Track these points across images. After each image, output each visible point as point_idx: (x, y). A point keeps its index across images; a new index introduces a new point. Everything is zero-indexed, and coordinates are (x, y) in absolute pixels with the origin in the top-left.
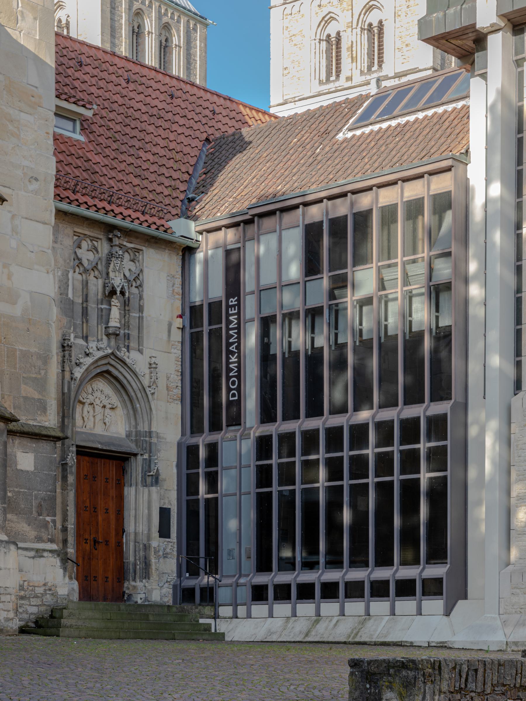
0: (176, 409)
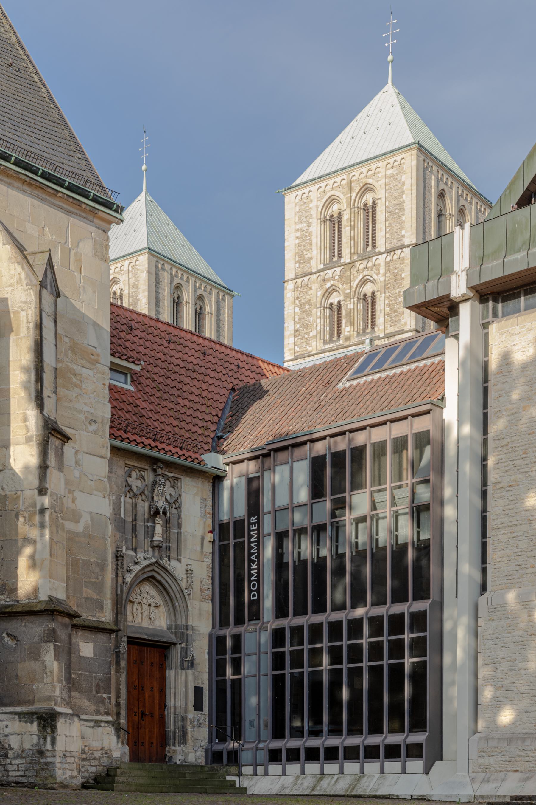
0: (207, 607)
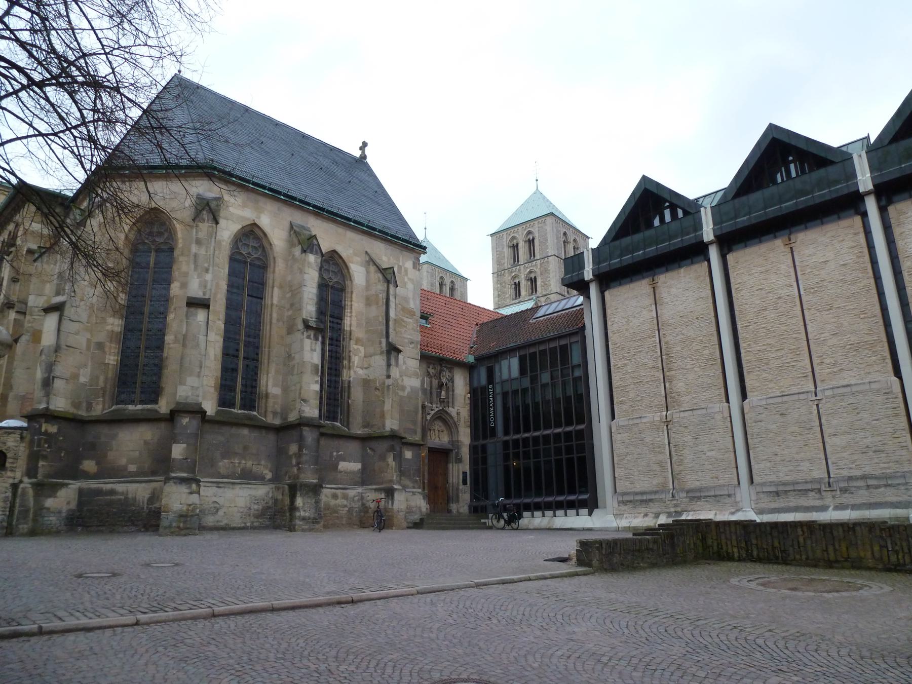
0: (468, 431)
